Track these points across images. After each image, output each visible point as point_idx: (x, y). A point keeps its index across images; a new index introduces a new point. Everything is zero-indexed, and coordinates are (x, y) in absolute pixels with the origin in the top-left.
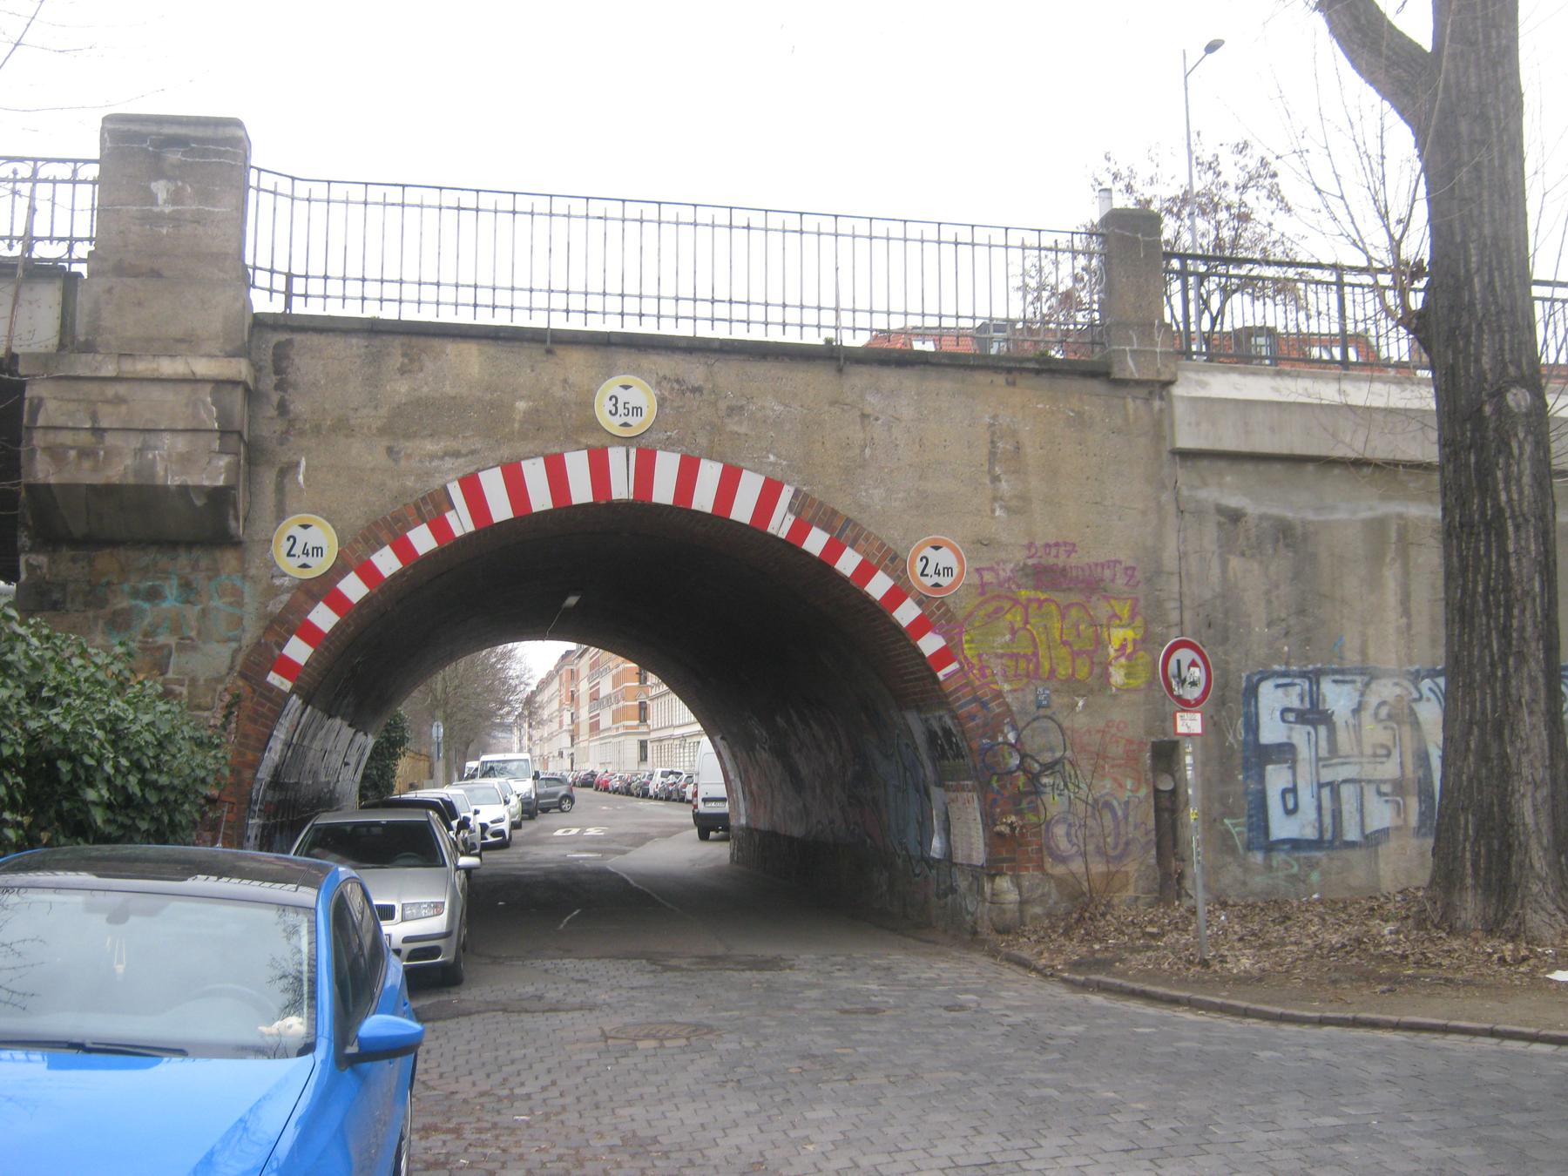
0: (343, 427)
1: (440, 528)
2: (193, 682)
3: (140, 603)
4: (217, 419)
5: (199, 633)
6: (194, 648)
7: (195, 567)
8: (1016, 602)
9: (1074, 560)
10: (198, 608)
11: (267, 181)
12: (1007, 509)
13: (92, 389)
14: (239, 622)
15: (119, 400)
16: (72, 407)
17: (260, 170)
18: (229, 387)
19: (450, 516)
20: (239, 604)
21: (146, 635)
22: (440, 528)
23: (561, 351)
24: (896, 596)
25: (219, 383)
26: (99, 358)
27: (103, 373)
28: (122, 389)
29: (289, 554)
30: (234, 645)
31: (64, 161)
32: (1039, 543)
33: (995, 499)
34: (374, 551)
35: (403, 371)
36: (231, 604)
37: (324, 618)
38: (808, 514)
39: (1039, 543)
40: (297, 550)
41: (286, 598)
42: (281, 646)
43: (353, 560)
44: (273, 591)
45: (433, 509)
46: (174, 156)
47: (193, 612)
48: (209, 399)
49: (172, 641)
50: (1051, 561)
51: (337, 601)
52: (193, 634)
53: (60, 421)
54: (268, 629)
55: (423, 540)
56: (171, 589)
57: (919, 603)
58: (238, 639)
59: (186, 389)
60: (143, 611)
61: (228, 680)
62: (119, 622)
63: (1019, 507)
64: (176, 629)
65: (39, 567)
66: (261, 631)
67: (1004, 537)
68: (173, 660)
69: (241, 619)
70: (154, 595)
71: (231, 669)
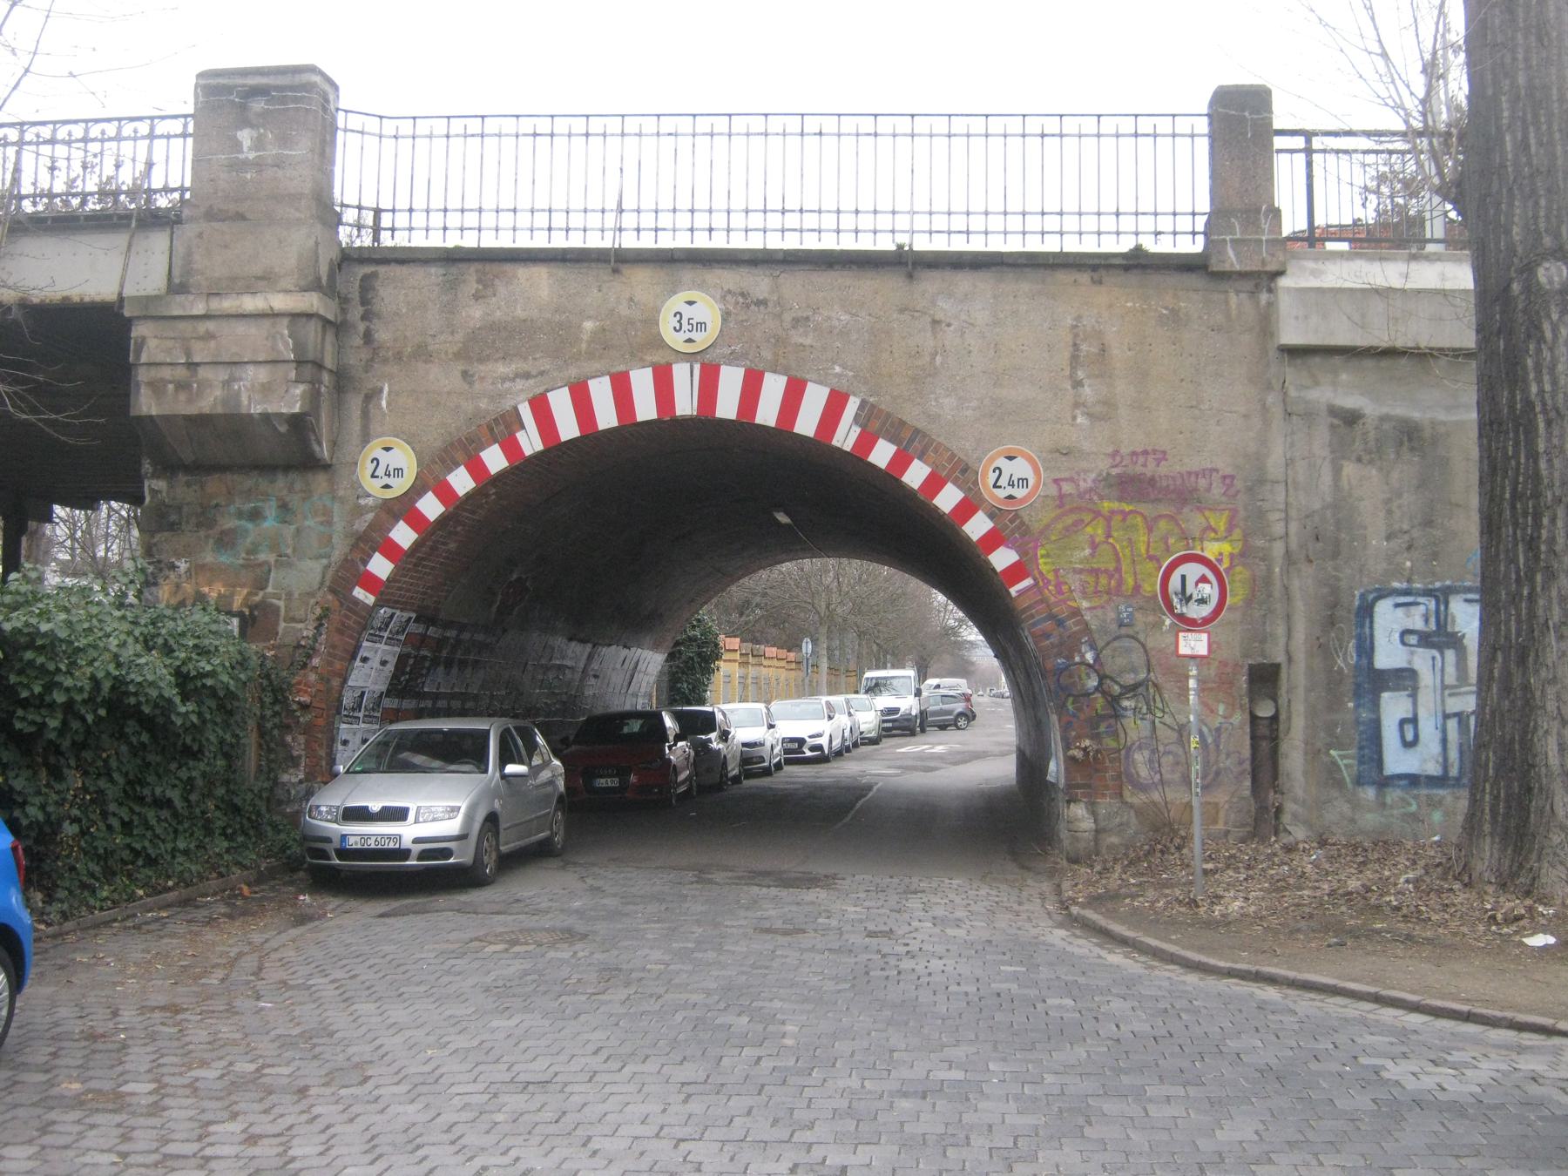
0: (422, 353)
1: (511, 447)
2: (289, 595)
3: (243, 523)
4: (294, 350)
5: (294, 550)
6: (290, 565)
8: (1098, 514)
9: (1163, 469)
10: (293, 527)
11: (354, 122)
12: (1090, 415)
14: (327, 540)
15: (209, 336)
16: (170, 344)
17: (346, 111)
18: (304, 320)
19: (520, 436)
20: (329, 523)
22: (511, 447)
23: (626, 270)
24: (966, 509)
25: (295, 316)
26: (191, 297)
27: (195, 312)
28: (211, 325)
29: (373, 476)
30: (325, 561)
31: (175, 117)
32: (1124, 451)
33: (1076, 405)
34: (450, 470)
35: (477, 297)
36: (322, 523)
37: (404, 535)
38: (875, 425)
39: (1124, 451)
40: (380, 472)
41: (370, 516)
42: (365, 563)
44: (359, 511)
45: (504, 429)
46: (258, 105)
48: (286, 332)
49: (272, 558)
50: (1139, 469)
51: (416, 520)
52: (289, 551)
53: (160, 358)
54: (354, 547)
55: (495, 460)
56: (271, 510)
57: (991, 516)
58: (328, 556)
59: (267, 323)
60: (247, 531)
61: (320, 593)
62: (226, 541)
63: (1103, 413)
64: (275, 547)
65: (160, 492)
66: (347, 550)
67: (1086, 446)
68: (272, 574)
69: (331, 537)
70: (255, 515)
71: (322, 583)
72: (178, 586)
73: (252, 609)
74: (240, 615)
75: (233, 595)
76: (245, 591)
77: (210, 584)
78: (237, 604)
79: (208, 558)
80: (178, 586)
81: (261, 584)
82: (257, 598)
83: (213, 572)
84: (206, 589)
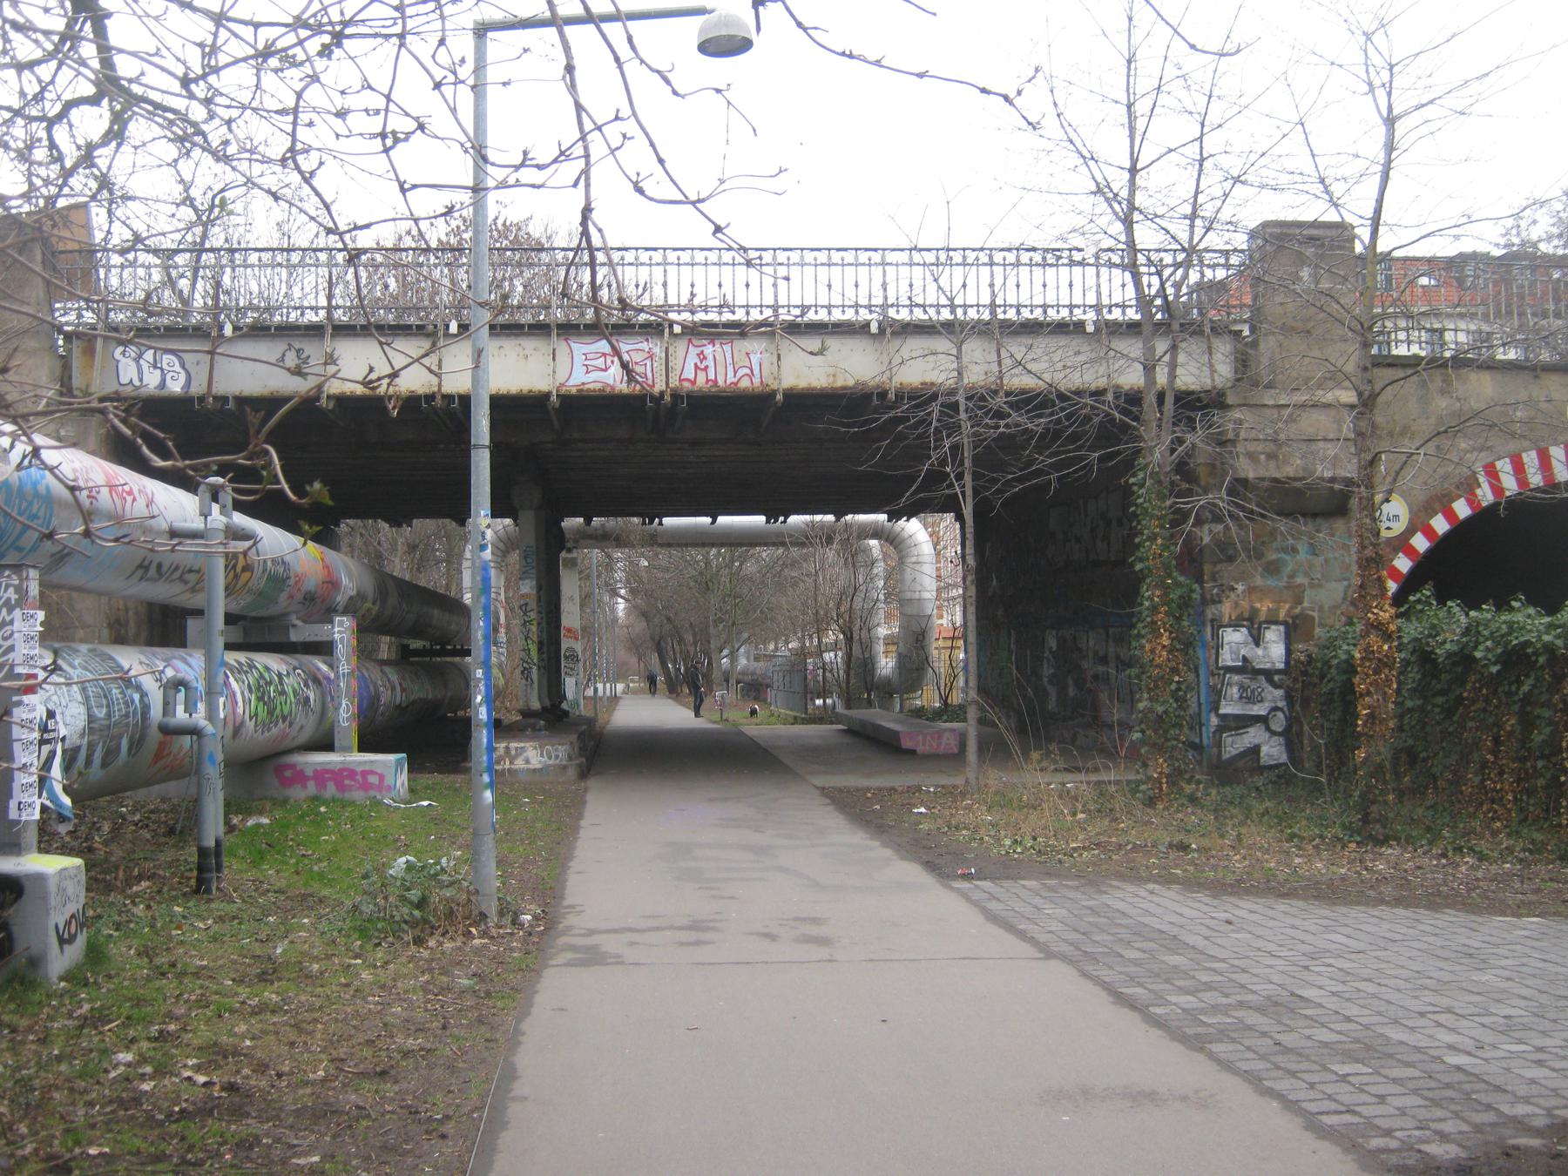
2: (1321, 609)
3: (1283, 555)
6: (1320, 586)
19: (1479, 492)
21: (1291, 577)
23: (1544, 376)
30: (1346, 583)
43: (1418, 523)
45: (1468, 487)
51: (1410, 551)
55: (1462, 509)
56: (1302, 548)
61: (1344, 606)
62: (1273, 569)
71: (1345, 599)
72: (1236, 604)
73: (1295, 617)
74: (1285, 623)
75: (1277, 609)
76: (1287, 606)
77: (1260, 601)
78: (1282, 615)
79: (1259, 581)
80: (1236, 604)
81: (1299, 601)
82: (1297, 611)
83: (1263, 592)
84: (1258, 605)
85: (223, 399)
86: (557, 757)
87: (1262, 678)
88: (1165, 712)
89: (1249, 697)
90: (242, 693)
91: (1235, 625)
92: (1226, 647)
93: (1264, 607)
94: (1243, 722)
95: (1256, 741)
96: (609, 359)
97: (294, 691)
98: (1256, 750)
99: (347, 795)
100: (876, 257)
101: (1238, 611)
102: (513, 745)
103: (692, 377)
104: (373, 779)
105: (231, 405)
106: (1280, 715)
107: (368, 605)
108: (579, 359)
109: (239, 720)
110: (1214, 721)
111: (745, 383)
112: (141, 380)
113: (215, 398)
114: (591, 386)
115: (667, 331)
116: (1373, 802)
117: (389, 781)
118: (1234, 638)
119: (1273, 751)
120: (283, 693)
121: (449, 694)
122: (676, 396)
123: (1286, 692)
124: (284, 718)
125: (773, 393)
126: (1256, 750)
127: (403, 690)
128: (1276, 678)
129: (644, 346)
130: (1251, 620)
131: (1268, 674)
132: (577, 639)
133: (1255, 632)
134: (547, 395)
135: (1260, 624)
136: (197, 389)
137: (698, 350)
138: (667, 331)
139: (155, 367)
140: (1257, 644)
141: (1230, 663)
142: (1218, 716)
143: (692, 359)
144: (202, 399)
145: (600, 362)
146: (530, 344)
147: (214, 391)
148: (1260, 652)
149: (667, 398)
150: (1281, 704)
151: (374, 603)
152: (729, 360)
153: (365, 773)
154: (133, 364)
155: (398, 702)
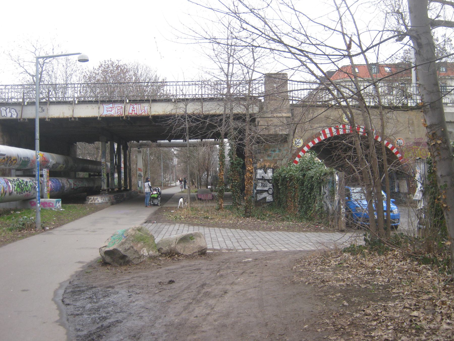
7: (281, 146)
8: (413, 148)
9: (423, 141)
12: (411, 132)
13: (267, 119)
15: (271, 121)
16: (264, 122)
19: (321, 137)
21: (274, 157)
24: (393, 148)
27: (269, 116)
28: (271, 119)
32: (417, 138)
33: (409, 131)
38: (378, 134)
39: (417, 138)
41: (295, 151)
45: (318, 137)
47: (280, 154)
50: (419, 141)
53: (263, 124)
54: (293, 156)
56: (277, 150)
57: (397, 149)
60: (273, 154)
62: (269, 156)
63: (413, 132)
64: (278, 156)
67: (411, 137)
72: (261, 164)
73: (275, 167)
74: (272, 168)
77: (267, 163)
78: (272, 166)
79: (266, 159)
80: (261, 164)
81: (276, 163)
83: (267, 161)
85: (24, 119)
86: (105, 200)
87: (267, 181)
88: (222, 189)
89: (263, 186)
90: (12, 186)
91: (260, 169)
92: (258, 174)
93: (267, 164)
94: (262, 192)
95: (266, 196)
96: (112, 109)
97: (31, 186)
98: (265, 198)
99: (45, 208)
100: (174, 84)
101: (261, 165)
102: (95, 197)
103: (131, 112)
104: (51, 204)
105: (26, 121)
106: (271, 190)
107: (61, 165)
108: (105, 109)
109: (10, 192)
110: (255, 191)
111: (143, 114)
112: (7, 115)
113: (23, 119)
114: (108, 115)
115: (125, 102)
116: (248, 208)
117: (55, 205)
118: (260, 172)
119: (269, 198)
120: (27, 185)
121: (96, 186)
122: (127, 117)
123: (273, 184)
124: (27, 191)
125: (149, 116)
126: (265, 198)
127: (74, 185)
128: (270, 181)
129: (120, 105)
130: (264, 168)
131: (268, 180)
132: (141, 171)
133: (265, 170)
134: (97, 118)
135: (266, 168)
136: (19, 117)
137: (133, 106)
138: (125, 102)
139: (10, 112)
140: (266, 173)
141: (259, 178)
142: (256, 190)
143: (131, 108)
144: (20, 119)
145: (110, 109)
146: (94, 106)
147: (23, 117)
148: (266, 175)
149: (124, 118)
150: (271, 187)
151: (63, 165)
152: (140, 108)
153: (49, 203)
154: (5, 112)
155: (72, 187)
